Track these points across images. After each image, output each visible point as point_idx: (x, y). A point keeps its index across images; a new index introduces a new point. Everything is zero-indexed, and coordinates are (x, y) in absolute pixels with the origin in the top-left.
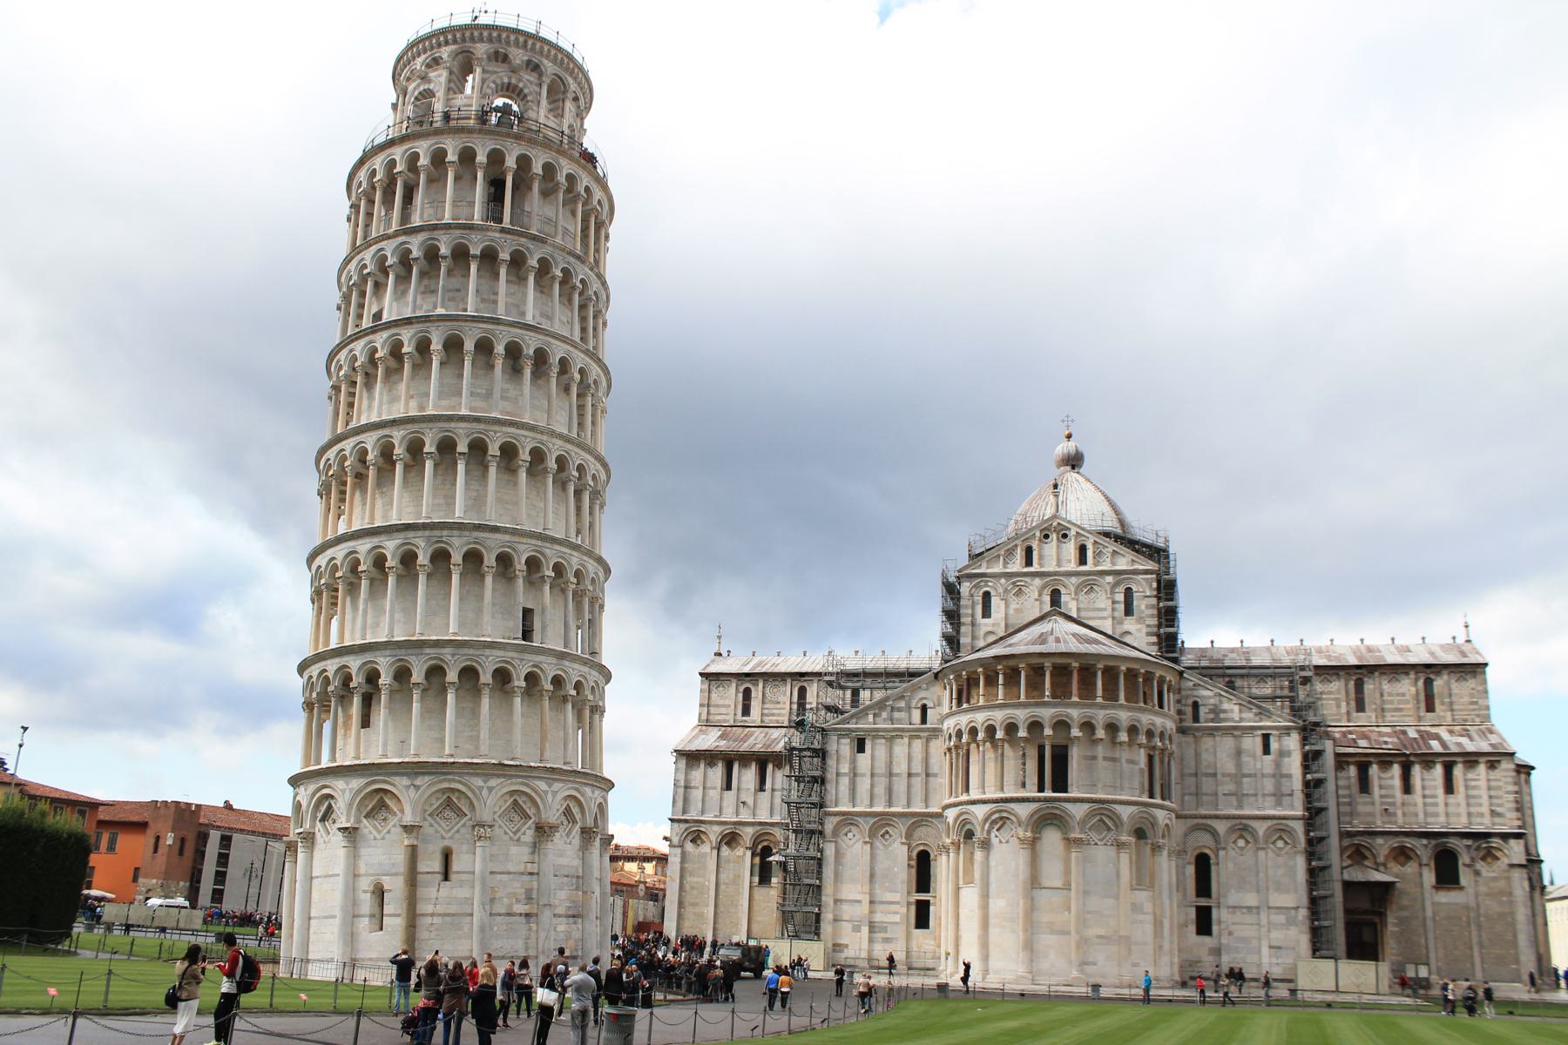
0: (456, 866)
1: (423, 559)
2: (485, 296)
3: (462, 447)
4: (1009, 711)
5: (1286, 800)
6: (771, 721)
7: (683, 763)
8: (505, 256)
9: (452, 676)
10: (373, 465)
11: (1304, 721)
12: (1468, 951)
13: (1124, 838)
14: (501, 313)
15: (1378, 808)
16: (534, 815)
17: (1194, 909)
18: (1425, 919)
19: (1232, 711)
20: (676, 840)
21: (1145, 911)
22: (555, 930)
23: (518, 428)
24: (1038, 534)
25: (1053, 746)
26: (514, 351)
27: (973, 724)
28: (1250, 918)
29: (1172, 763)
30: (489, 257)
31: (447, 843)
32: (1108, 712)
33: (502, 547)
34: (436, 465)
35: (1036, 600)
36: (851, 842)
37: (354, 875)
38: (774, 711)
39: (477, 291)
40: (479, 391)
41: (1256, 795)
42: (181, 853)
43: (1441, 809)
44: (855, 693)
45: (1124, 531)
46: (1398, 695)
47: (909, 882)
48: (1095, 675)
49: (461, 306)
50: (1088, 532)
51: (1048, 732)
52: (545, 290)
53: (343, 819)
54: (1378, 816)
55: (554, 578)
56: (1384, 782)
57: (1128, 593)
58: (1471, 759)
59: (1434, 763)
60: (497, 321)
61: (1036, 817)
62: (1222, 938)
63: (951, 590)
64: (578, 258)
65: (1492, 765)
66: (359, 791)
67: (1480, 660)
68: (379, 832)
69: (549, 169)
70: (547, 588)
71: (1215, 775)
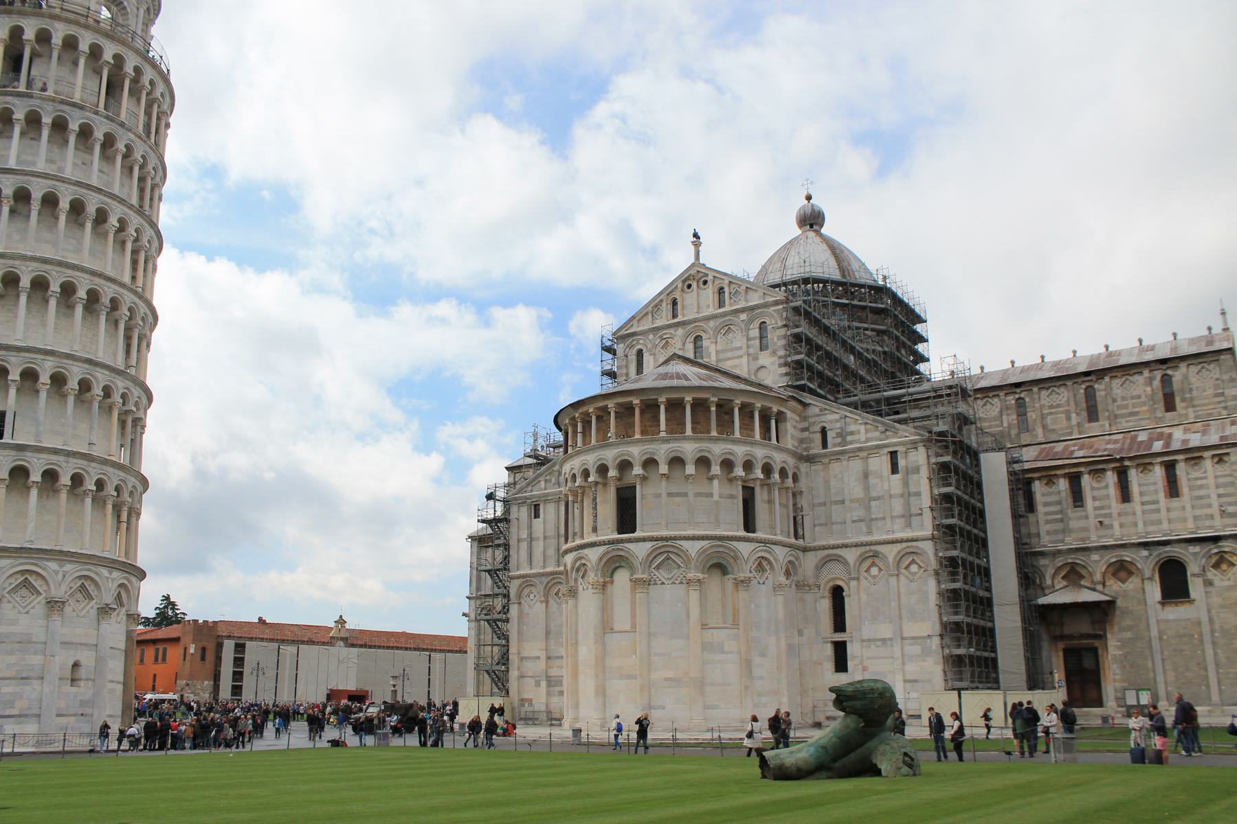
4: (583, 458)
5: (915, 520)
7: (476, 544)
12: (1202, 672)
14: (68, 173)
15: (1093, 521)
18: (1150, 640)
19: (859, 432)
20: (473, 616)
21: (726, 648)
24: (680, 285)
36: (534, 601)
41: (884, 518)
42: (203, 659)
45: (844, 276)
46: (1132, 398)
48: (659, 407)
51: (612, 473)
54: (1093, 530)
56: (1097, 493)
57: (762, 326)
58: (1194, 455)
61: (605, 560)
65: (1220, 459)
71: (843, 502)
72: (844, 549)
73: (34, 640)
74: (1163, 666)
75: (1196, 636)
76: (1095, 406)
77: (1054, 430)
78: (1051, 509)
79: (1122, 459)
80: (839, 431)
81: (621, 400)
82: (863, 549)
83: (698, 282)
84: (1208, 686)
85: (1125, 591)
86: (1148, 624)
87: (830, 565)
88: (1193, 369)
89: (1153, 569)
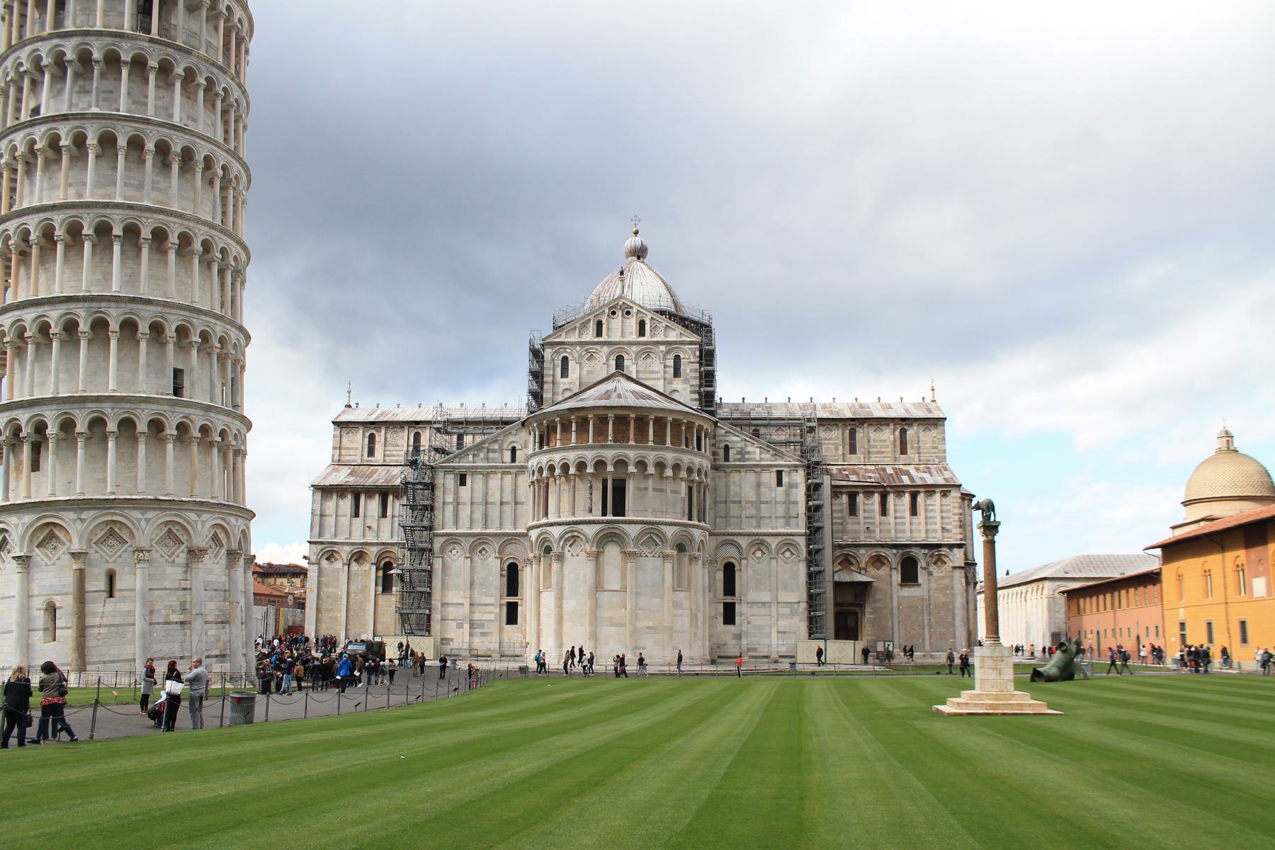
0: (118, 585)
1: (84, 326)
2: (136, 99)
3: (118, 231)
4: (580, 452)
5: (793, 521)
6: (392, 461)
7: (319, 495)
8: (153, 63)
9: (112, 426)
10: (36, 244)
11: (808, 461)
12: (921, 631)
13: (668, 551)
14: (150, 114)
15: (862, 527)
16: (187, 541)
17: (722, 605)
19: (754, 452)
20: (313, 559)
21: (684, 607)
22: (206, 634)
23: (167, 215)
24: (607, 311)
25: (613, 480)
26: (163, 149)
27: (551, 463)
28: (763, 611)
29: (707, 492)
30: (139, 64)
31: (111, 566)
32: (657, 453)
33: (155, 316)
34: (94, 246)
35: (604, 364)
36: (458, 555)
37: (28, 596)
38: (395, 453)
39: (129, 93)
40: (132, 182)
41: (771, 517)
43: (907, 527)
44: (460, 438)
45: (677, 311)
46: (881, 441)
47: (501, 588)
48: (648, 424)
49: (114, 106)
50: (646, 310)
51: (610, 468)
52: (191, 96)
53: (17, 549)
54: (862, 533)
55: (201, 344)
56: (867, 507)
57: (677, 359)
58: (930, 489)
59: (904, 492)
60: (147, 121)
62: (743, 626)
63: (537, 355)
64: (220, 68)
66: (31, 525)
67: (941, 416)
68: (50, 559)
70: (194, 352)
71: (740, 502)
72: (739, 537)
74: (899, 626)
75: (920, 607)
76: (855, 444)
80: (739, 450)
82: (754, 538)
83: (623, 311)
84: (924, 640)
85: (879, 576)
86: (892, 598)
88: (922, 428)
89: (898, 563)
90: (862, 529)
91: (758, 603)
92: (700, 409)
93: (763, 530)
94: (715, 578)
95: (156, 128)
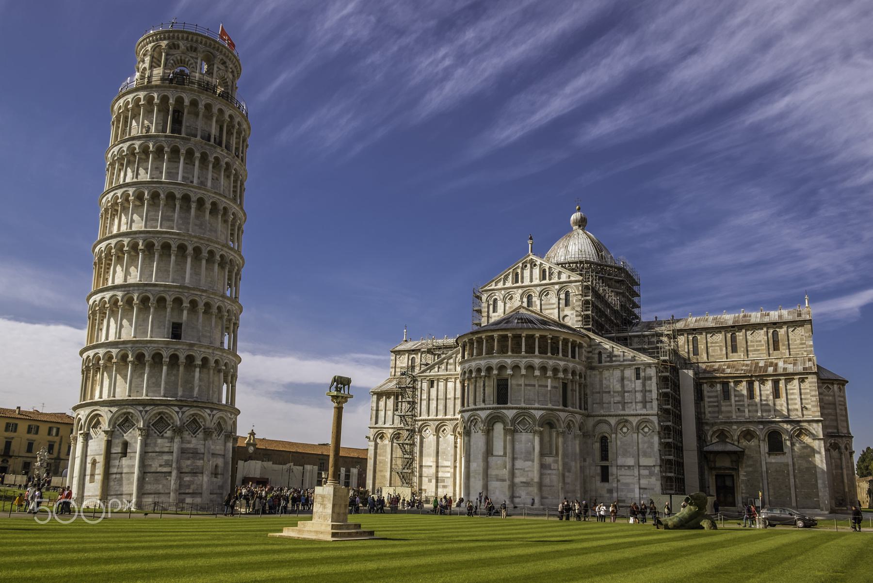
5: (648, 405)
12: (788, 491)
16: (173, 423)
18: (762, 472)
21: (552, 468)
23: (170, 235)
28: (628, 472)
32: (528, 359)
41: (632, 403)
46: (757, 342)
51: (495, 372)
54: (734, 412)
57: (567, 294)
69: (194, 103)
70: (185, 312)
71: (609, 392)
73: (199, 452)
77: (713, 355)
78: (712, 400)
79: (752, 376)
81: (501, 333)
82: (620, 418)
84: (790, 498)
87: (601, 424)
89: (765, 436)
90: (734, 410)
91: (626, 466)
92: (582, 328)
93: (627, 412)
94: (593, 448)
95: (166, 186)
